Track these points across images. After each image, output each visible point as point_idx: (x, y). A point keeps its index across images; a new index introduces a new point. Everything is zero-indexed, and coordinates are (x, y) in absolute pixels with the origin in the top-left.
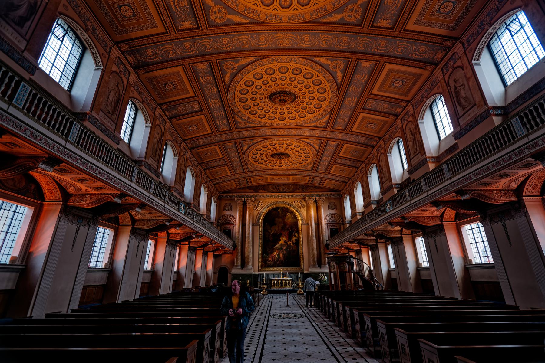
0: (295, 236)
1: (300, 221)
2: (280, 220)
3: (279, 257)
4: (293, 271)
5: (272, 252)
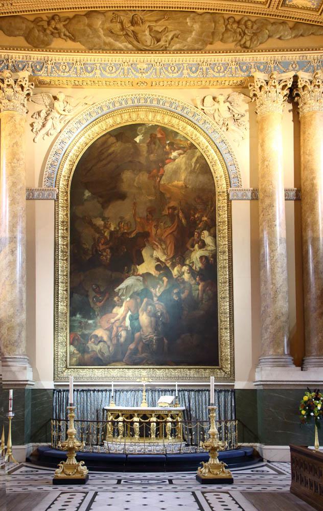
0: (203, 245)
1: (221, 185)
2: (143, 177)
3: (136, 327)
4: (194, 379)
5: (108, 306)
